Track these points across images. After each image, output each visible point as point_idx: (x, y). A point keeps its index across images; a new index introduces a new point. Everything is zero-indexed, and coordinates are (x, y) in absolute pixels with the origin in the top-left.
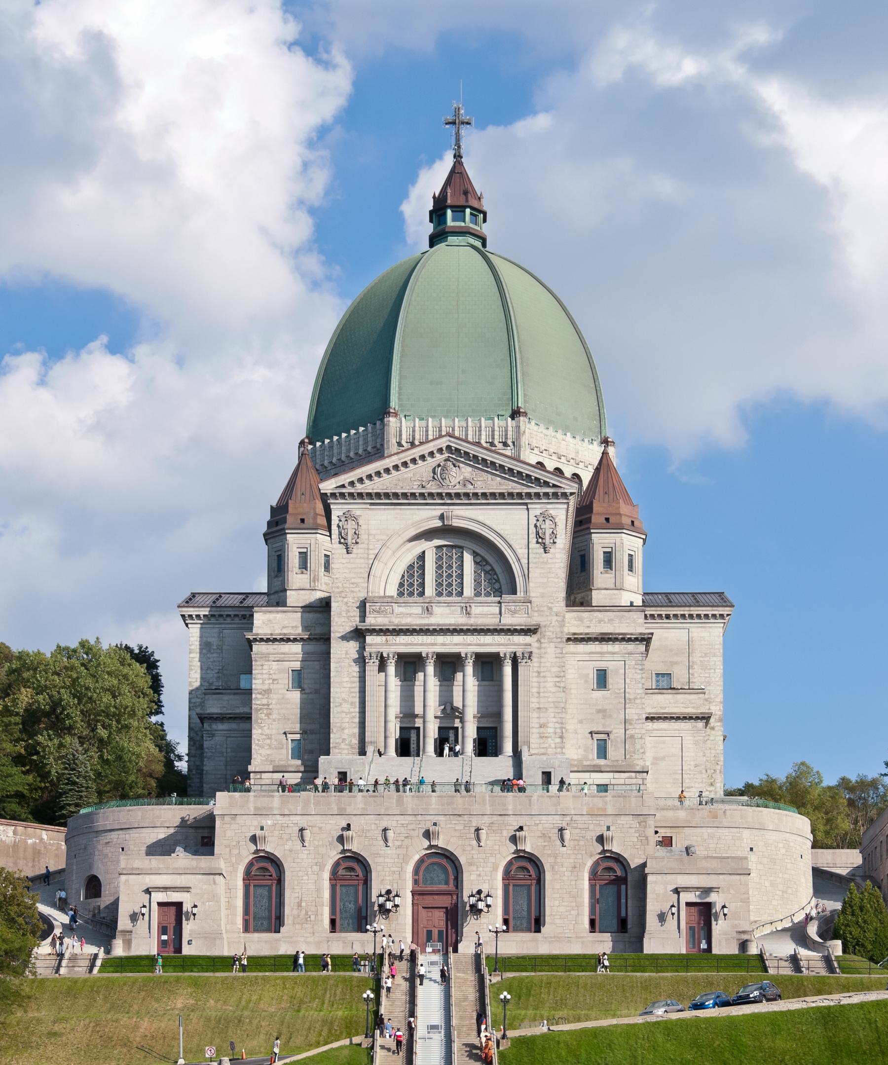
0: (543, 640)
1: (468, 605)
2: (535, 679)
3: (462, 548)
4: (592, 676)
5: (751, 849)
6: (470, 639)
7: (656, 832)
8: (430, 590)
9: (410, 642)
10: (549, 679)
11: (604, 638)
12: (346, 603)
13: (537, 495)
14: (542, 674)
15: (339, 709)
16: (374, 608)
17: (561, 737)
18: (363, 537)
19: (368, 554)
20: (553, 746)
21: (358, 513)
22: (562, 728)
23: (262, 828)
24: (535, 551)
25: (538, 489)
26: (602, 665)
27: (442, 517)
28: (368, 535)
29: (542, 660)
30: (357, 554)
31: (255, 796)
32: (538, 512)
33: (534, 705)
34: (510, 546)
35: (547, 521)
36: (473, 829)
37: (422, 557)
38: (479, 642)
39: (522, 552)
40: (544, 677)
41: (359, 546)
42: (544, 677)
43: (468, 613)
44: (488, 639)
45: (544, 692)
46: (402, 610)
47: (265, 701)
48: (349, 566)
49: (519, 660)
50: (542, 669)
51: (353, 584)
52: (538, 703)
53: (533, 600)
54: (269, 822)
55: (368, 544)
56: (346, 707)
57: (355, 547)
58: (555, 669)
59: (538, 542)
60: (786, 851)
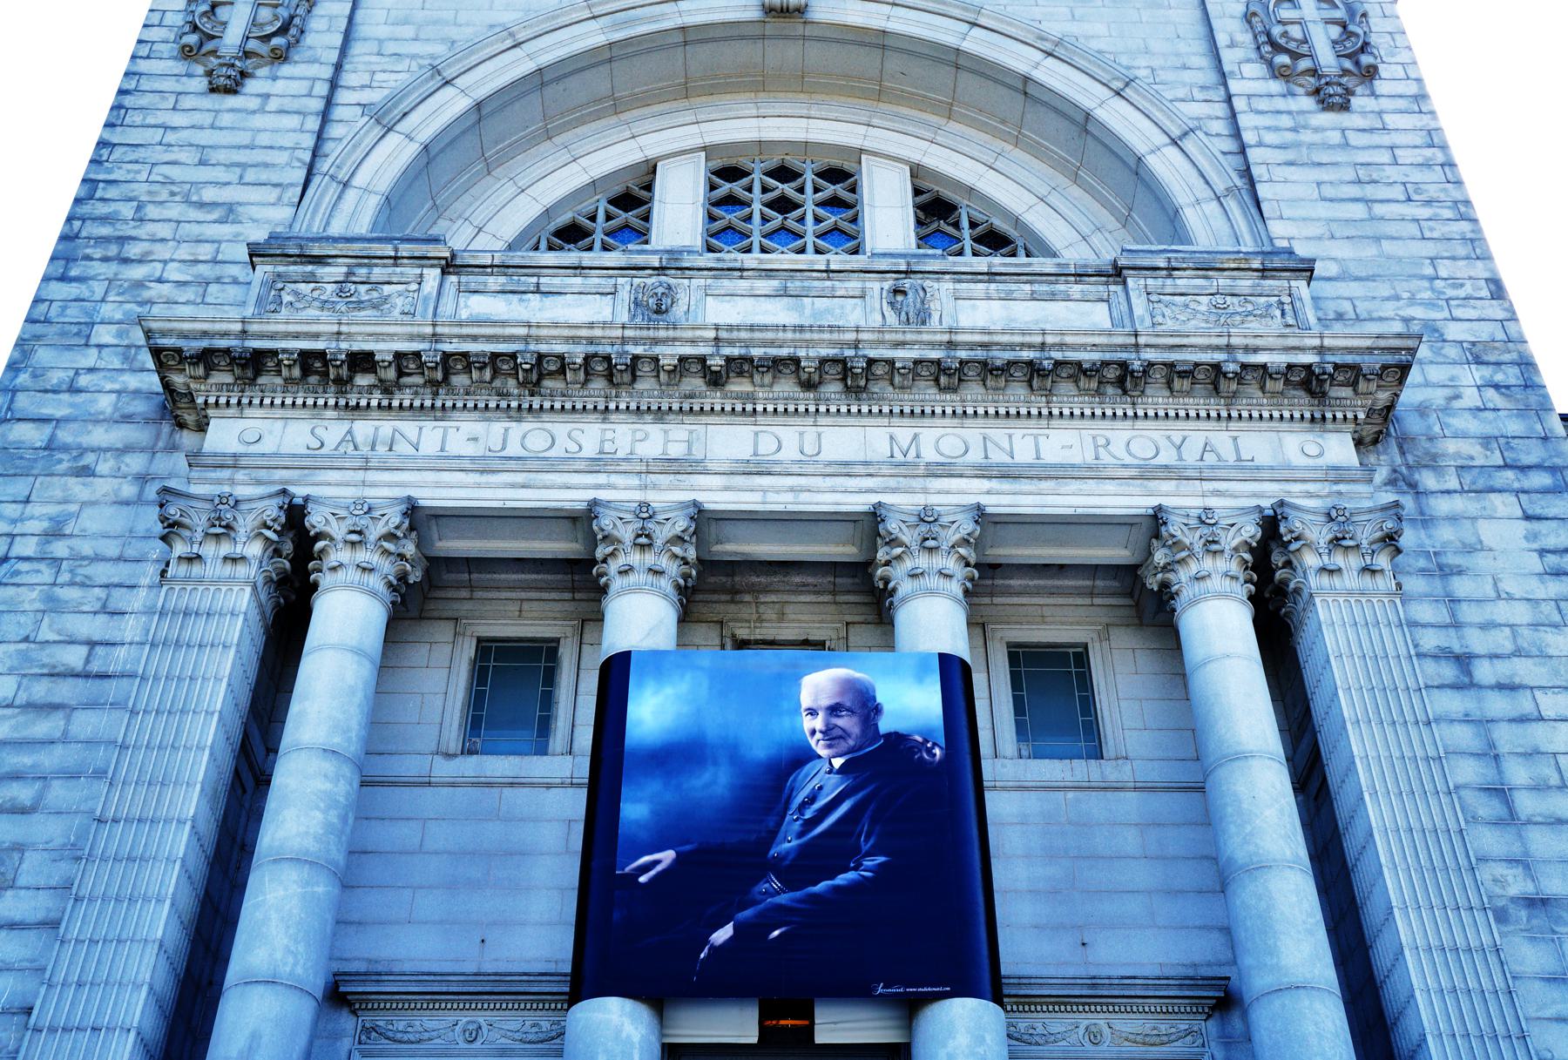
0: (1428, 480)
1: (907, 283)
9: (513, 449)
12: (139, 284)
14: (1484, 672)
16: (304, 288)
19: (329, 102)
24: (1263, 105)
29: (1461, 587)
30: (267, 96)
38: (997, 457)
40: (1508, 687)
41: (286, 70)
42: (1508, 687)
45: (1540, 787)
48: (204, 137)
49: (1310, 560)
50: (1477, 642)
51: (201, 205)
52: (1523, 862)
55: (338, 67)
57: (263, 72)
59: (1277, 73)
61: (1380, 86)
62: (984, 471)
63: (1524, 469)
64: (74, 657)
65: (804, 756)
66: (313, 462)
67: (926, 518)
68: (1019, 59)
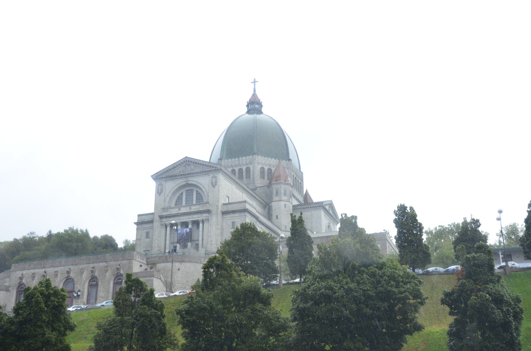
0: (212, 215)
2: (210, 227)
3: (193, 190)
4: (231, 224)
5: (179, 269)
6: (190, 217)
7: (141, 266)
8: (184, 204)
10: (214, 226)
11: (234, 212)
13: (210, 170)
14: (212, 225)
15: (154, 242)
17: (217, 244)
18: (164, 190)
19: (165, 195)
20: (214, 247)
21: (163, 183)
22: (217, 241)
23: (22, 274)
25: (211, 169)
26: (232, 221)
27: (185, 181)
28: (165, 189)
31: (22, 264)
32: (212, 176)
33: (209, 235)
34: (204, 187)
35: (214, 178)
36: (80, 270)
37: (182, 194)
39: (207, 188)
40: (212, 226)
41: (163, 193)
42: (212, 226)
43: (190, 209)
44: (195, 216)
46: (173, 210)
47: (139, 242)
51: (160, 204)
53: (209, 202)
54: (25, 272)
56: (156, 241)
58: (215, 223)
59: (212, 185)
60: (195, 269)
61: (217, 185)
62: (192, 218)
63: (216, 213)
64: (159, 231)
65: (184, 233)
66: (166, 221)
67: (190, 221)
68: (199, 185)
